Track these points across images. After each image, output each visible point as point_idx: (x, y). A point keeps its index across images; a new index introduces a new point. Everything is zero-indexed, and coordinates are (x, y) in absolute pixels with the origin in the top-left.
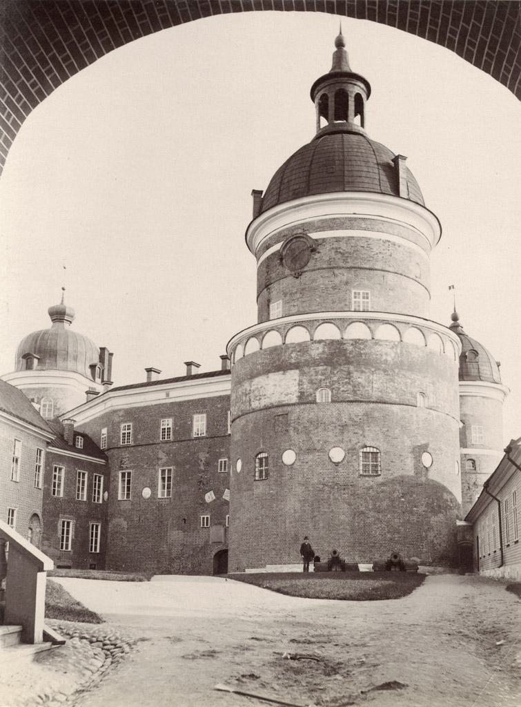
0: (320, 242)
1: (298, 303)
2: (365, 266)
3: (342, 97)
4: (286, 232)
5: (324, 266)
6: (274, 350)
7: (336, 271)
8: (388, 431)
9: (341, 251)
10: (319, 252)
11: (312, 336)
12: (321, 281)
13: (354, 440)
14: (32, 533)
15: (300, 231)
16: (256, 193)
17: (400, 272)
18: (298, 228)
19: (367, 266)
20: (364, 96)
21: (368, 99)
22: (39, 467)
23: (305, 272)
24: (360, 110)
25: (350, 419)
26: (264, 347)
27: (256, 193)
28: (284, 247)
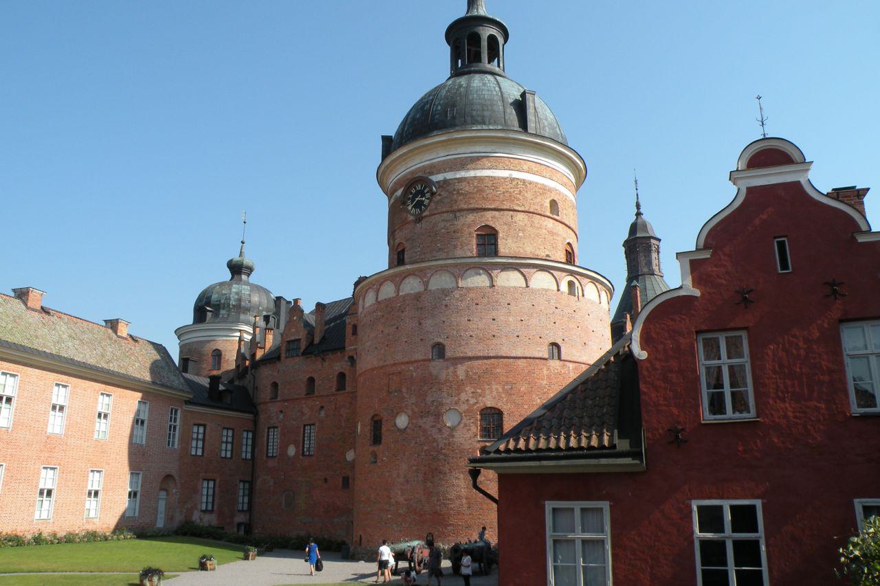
0: (441, 184)
1: (419, 249)
2: (489, 207)
3: (475, 39)
4: (409, 177)
5: (444, 210)
6: (389, 302)
7: (458, 214)
8: (512, 388)
9: (463, 192)
10: (440, 195)
11: (426, 284)
12: (442, 225)
13: (472, 401)
14: (167, 495)
15: (420, 174)
16: (386, 140)
17: (532, 210)
18: (419, 172)
19: (493, 207)
20: (501, 40)
21: (506, 41)
22: (175, 427)
23: (426, 216)
24: (494, 52)
25: (467, 375)
26: (379, 300)
27: (386, 140)
28: (405, 193)
